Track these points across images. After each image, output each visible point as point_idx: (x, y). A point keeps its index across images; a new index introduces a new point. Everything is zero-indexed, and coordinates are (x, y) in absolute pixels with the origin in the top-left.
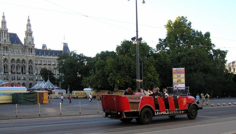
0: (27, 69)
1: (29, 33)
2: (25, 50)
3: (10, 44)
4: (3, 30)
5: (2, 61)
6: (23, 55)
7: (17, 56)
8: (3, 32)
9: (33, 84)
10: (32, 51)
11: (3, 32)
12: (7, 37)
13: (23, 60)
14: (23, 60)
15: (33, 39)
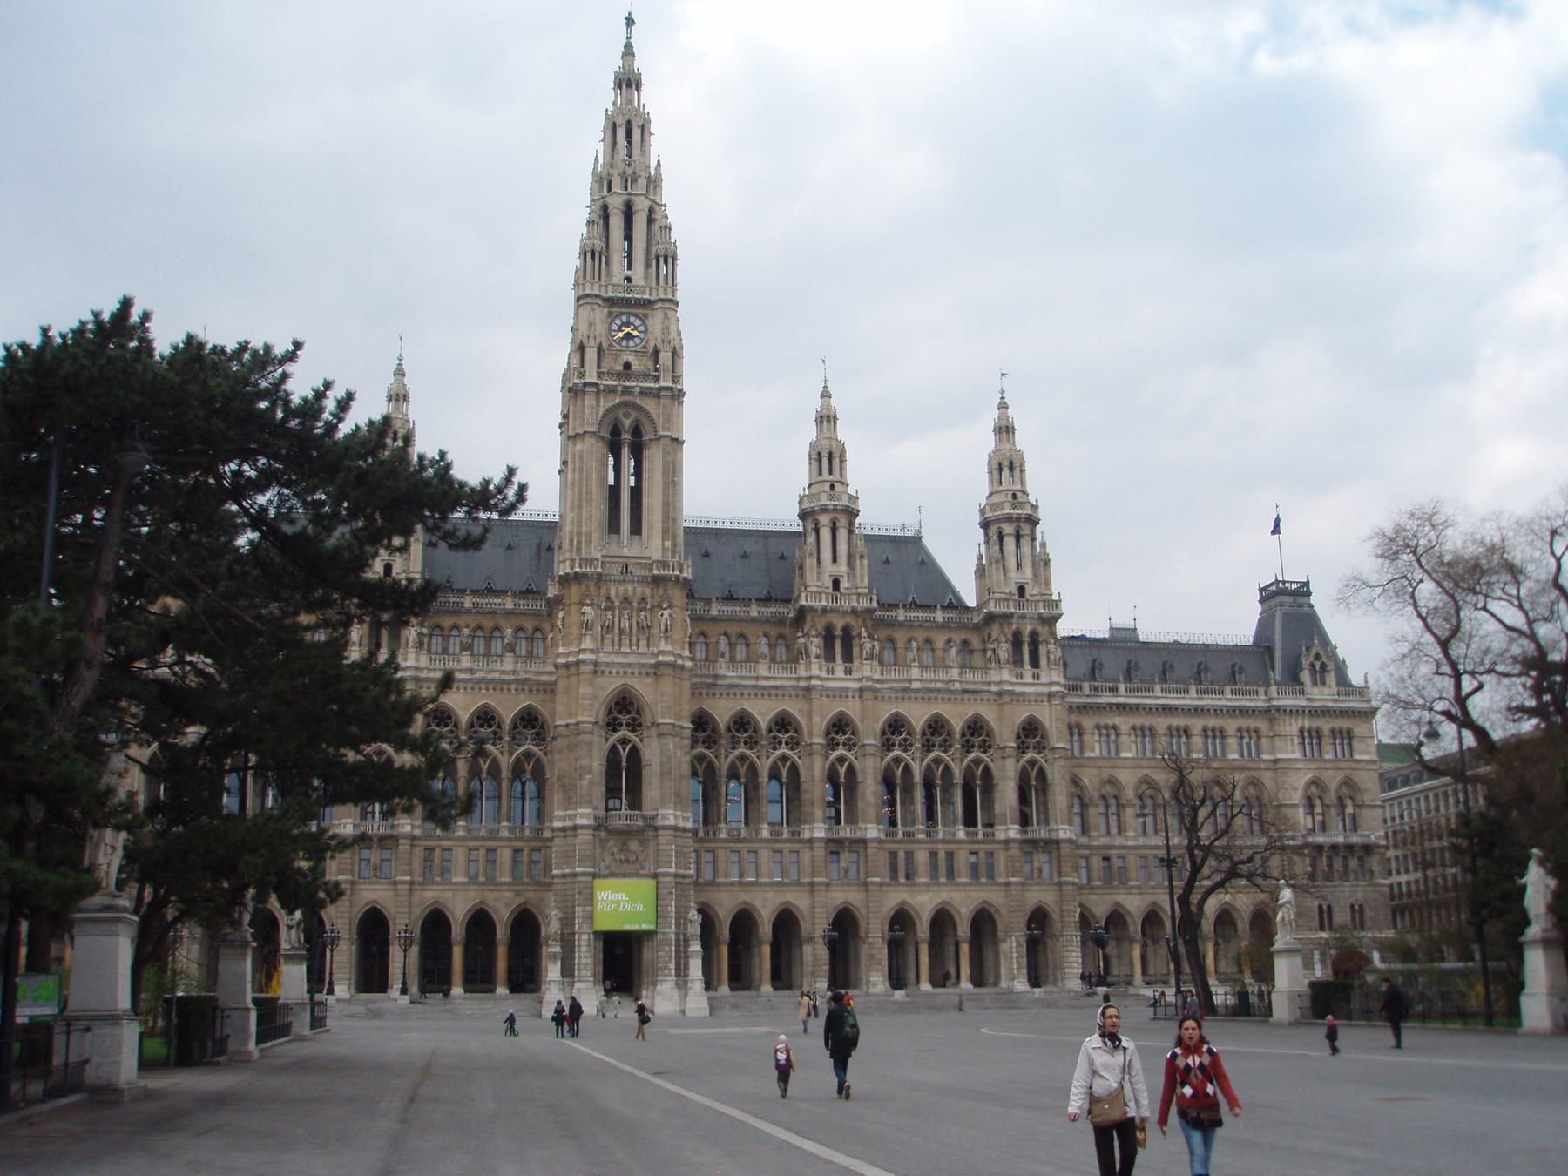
0: (1007, 795)
1: (1009, 519)
2: (985, 651)
3: (875, 604)
4: (824, 510)
5: (819, 740)
6: (973, 679)
7: (927, 694)
8: (825, 520)
9: (1055, 916)
10: (1042, 650)
11: (825, 520)
12: (850, 557)
13: (976, 727)
14: (976, 727)
15: (1047, 563)
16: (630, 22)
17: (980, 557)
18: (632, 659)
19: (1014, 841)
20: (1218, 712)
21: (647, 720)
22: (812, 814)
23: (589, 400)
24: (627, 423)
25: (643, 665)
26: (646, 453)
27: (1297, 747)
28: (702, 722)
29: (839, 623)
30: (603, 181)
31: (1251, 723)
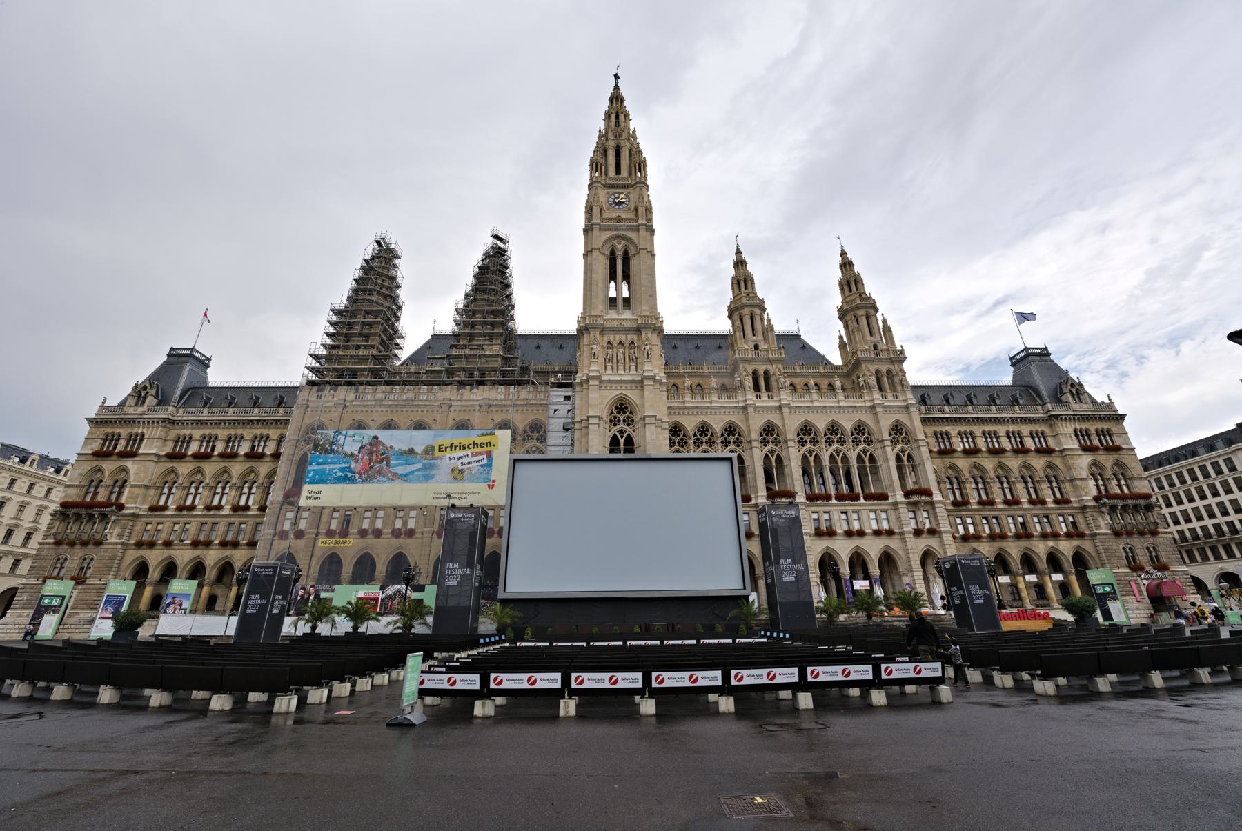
5: (755, 436)
8: (746, 312)
10: (896, 380)
11: (746, 312)
16: (617, 77)
17: (841, 337)
18: (625, 378)
19: (902, 503)
20: (1014, 420)
21: (637, 418)
22: (756, 487)
23: (596, 232)
24: (619, 247)
25: (633, 381)
26: (632, 262)
27: (1076, 442)
28: (676, 430)
29: (761, 369)
30: (602, 137)
31: (1039, 428)
